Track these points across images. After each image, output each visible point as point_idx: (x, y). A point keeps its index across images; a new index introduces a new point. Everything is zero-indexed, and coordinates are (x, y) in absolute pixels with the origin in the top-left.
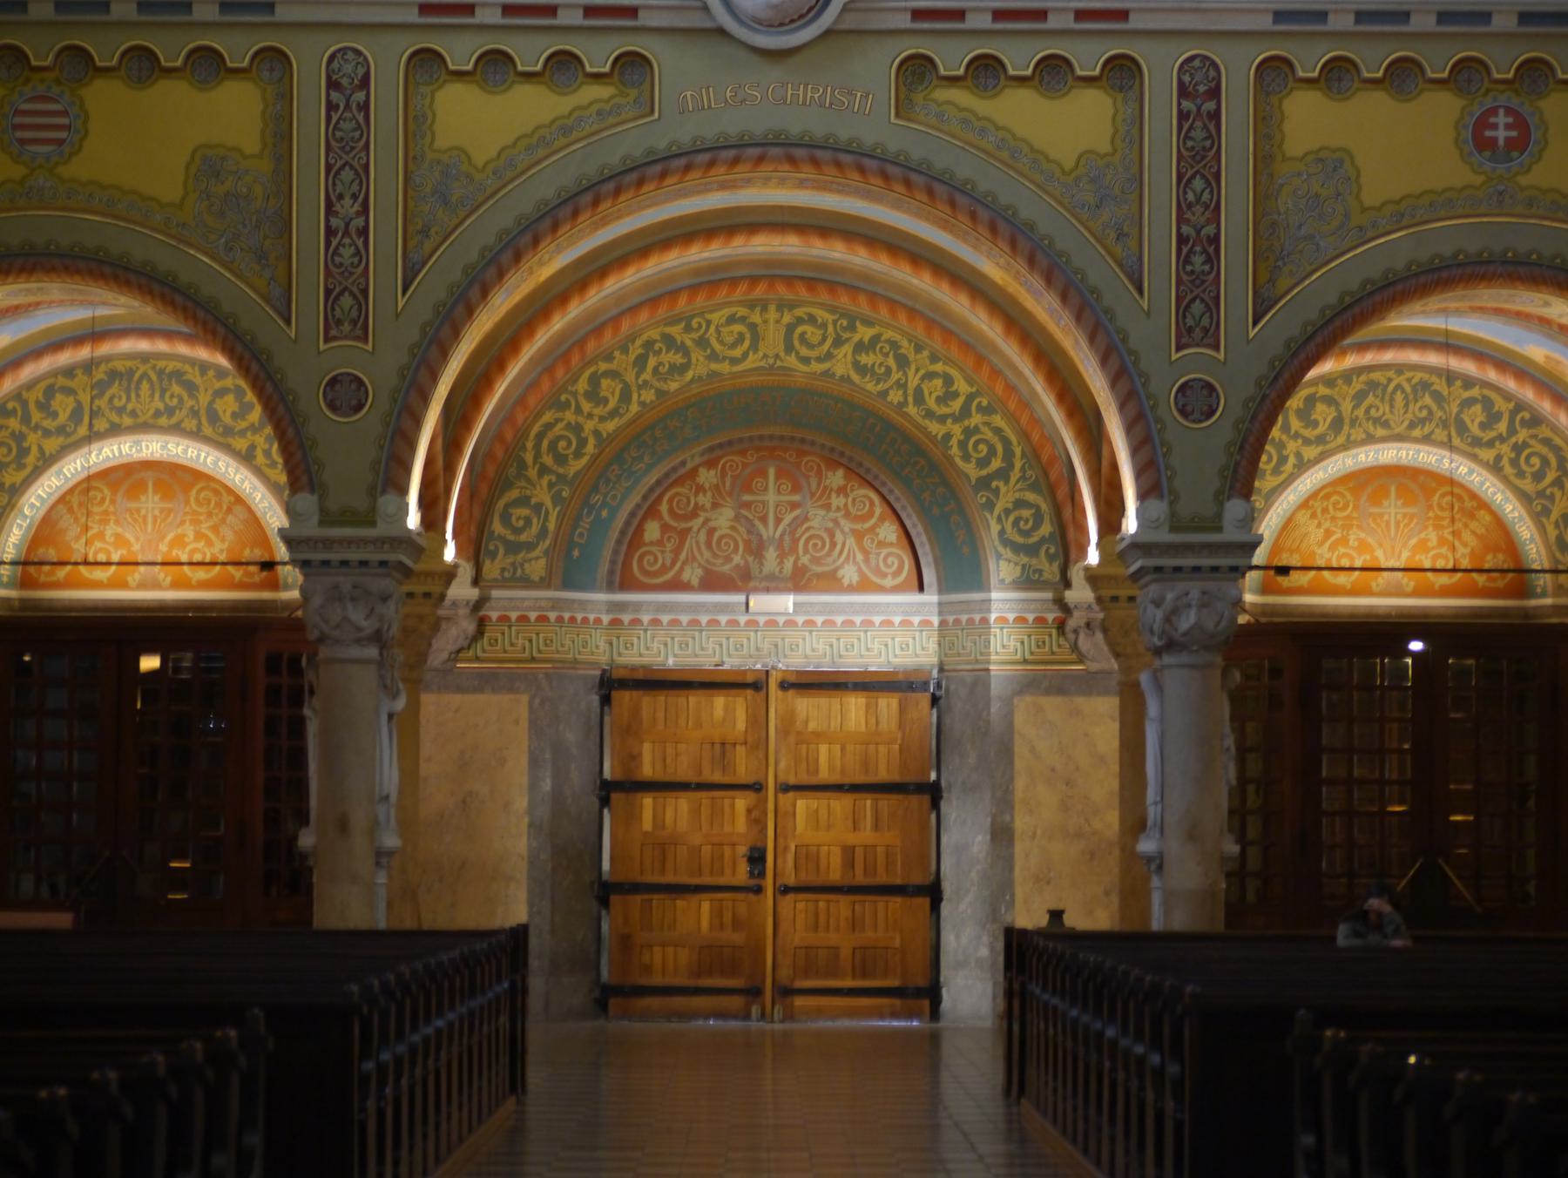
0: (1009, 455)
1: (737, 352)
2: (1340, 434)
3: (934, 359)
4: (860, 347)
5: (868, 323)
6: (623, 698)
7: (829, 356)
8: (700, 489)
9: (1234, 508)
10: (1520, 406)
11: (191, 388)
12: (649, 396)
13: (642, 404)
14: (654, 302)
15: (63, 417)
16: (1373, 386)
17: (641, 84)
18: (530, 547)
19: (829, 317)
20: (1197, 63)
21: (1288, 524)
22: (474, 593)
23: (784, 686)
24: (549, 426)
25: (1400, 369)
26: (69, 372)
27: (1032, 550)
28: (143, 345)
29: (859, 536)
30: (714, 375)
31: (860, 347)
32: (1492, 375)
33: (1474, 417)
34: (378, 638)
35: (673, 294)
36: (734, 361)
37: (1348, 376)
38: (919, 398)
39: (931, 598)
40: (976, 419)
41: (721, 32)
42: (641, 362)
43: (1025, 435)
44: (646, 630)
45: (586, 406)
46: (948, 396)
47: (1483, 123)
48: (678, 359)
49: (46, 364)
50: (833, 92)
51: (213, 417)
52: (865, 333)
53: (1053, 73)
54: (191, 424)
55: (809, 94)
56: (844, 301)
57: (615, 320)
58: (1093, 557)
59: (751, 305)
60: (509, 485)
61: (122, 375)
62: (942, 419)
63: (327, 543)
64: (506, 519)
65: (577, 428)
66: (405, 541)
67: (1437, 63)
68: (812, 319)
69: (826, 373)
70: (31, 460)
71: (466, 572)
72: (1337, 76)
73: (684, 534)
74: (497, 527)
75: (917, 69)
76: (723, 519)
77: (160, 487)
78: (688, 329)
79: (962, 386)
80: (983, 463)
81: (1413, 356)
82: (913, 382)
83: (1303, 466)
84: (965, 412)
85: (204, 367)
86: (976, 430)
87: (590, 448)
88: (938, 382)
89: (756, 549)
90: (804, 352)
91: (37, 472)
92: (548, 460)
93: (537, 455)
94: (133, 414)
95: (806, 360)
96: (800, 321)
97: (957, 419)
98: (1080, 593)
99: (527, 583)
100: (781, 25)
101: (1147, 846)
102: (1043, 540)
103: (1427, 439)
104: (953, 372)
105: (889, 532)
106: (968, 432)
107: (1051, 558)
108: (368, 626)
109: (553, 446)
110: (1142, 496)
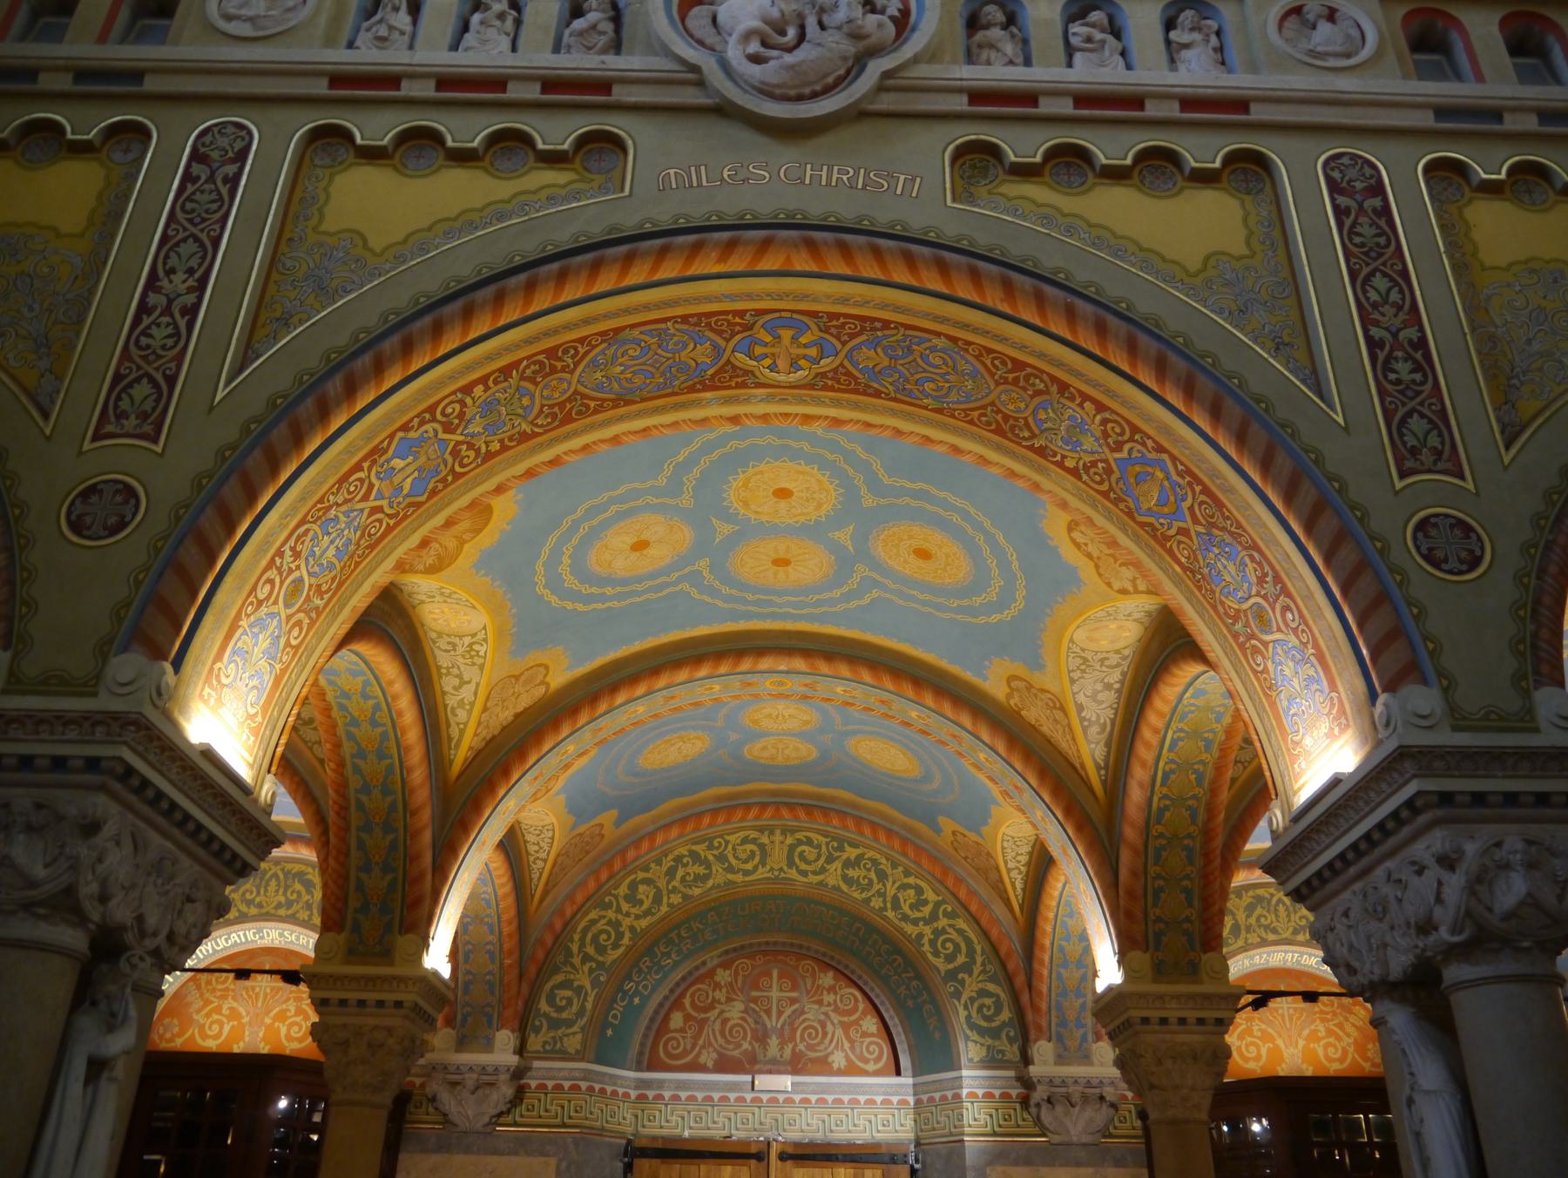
0: (971, 952)
1: (749, 866)
3: (907, 874)
4: (848, 864)
5: (854, 845)
6: (644, 1165)
7: (823, 870)
8: (717, 986)
12: (676, 899)
13: (669, 905)
14: (683, 821)
16: (1259, 899)
17: (611, 170)
18: (569, 1023)
19: (823, 840)
20: (1345, 160)
22: (514, 1060)
23: (783, 1157)
24: (593, 922)
27: (994, 1034)
29: (846, 1027)
30: (731, 882)
31: (848, 864)
35: (699, 816)
36: (746, 873)
38: (896, 905)
39: (907, 1080)
40: (943, 922)
42: (671, 873)
43: (985, 934)
44: (666, 1105)
45: (625, 907)
46: (920, 903)
48: (701, 870)
50: (867, 174)
52: (852, 853)
54: (303, 915)
55: (835, 176)
59: (761, 830)
60: (556, 971)
62: (915, 922)
64: (551, 1001)
65: (616, 924)
68: (809, 842)
69: (821, 883)
73: (702, 1023)
74: (544, 1006)
76: (735, 1011)
78: (711, 847)
79: (930, 895)
80: (950, 958)
82: (891, 891)
84: (934, 917)
86: (944, 931)
87: (626, 941)
88: (912, 892)
89: (762, 1038)
90: (803, 867)
92: (591, 950)
93: (582, 945)
94: (260, 906)
95: (804, 873)
96: (800, 842)
97: (927, 922)
99: (564, 1056)
102: (1004, 1025)
104: (922, 884)
105: (871, 1024)
106: (937, 933)
107: (1011, 1040)
109: (595, 939)
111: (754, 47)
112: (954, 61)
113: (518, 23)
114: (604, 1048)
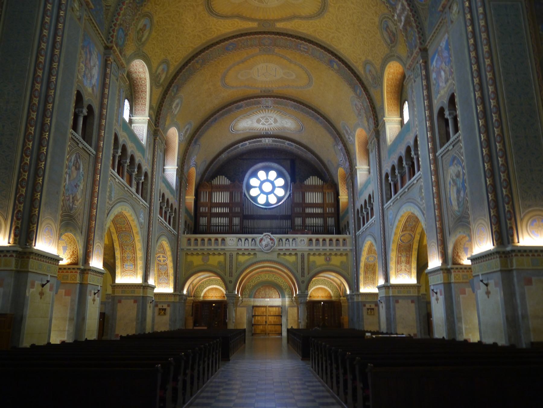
2: (315, 284)
9: (306, 291)
10: (330, 282)
11: (218, 281)
15: (207, 284)
16: (318, 280)
21: (311, 292)
22: (242, 299)
25: (320, 279)
26: (207, 280)
27: (289, 295)
28: (214, 278)
32: (328, 279)
33: (327, 283)
34: (233, 303)
37: (316, 280)
39: (281, 299)
40: (284, 283)
41: (262, 251)
42: (256, 279)
43: (289, 285)
46: (282, 281)
47: (326, 258)
49: (206, 279)
51: (220, 284)
52: (275, 276)
53: (290, 254)
56: (273, 273)
57: (254, 275)
58: (294, 296)
61: (212, 280)
63: (229, 295)
66: (236, 295)
67: (322, 253)
70: (204, 287)
71: (241, 297)
72: (314, 254)
73: (260, 294)
74: (244, 293)
75: (279, 254)
76: (263, 292)
77: (215, 290)
79: (283, 281)
81: (321, 278)
83: (312, 287)
85: (219, 279)
89: (266, 295)
91: (205, 288)
98: (293, 299)
99: (246, 298)
101: (299, 321)
103: (323, 285)
105: (277, 293)
108: (232, 302)
110: (298, 290)
114: (250, 297)
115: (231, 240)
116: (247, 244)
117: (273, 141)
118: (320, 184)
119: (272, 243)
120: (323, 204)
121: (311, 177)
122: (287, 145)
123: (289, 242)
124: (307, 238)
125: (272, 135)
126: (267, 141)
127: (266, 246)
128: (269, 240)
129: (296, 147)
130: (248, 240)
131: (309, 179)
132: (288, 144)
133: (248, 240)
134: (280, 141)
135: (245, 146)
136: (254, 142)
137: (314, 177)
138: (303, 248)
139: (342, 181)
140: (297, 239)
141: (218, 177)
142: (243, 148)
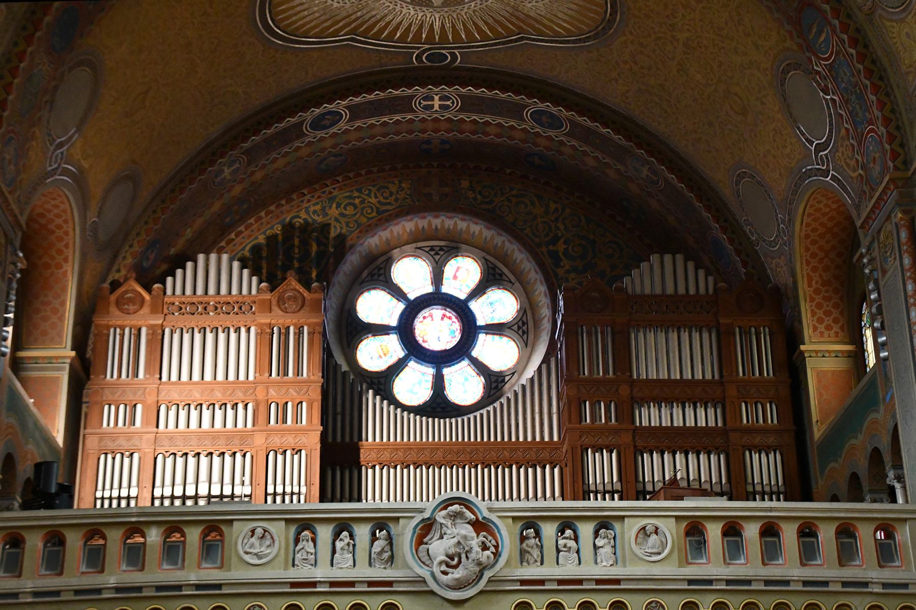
20: (653, 605)
41: (432, 593)
100: (460, 588)
111: (444, 568)
112: (516, 568)
113: (354, 546)
115: (259, 531)
116: (344, 558)
117: (469, 104)
118: (702, 291)
119: (485, 548)
120: (721, 383)
121: (655, 258)
122: (529, 124)
123: (576, 539)
124: (677, 518)
125: (457, 68)
126: (437, 103)
127: (452, 561)
128: (468, 530)
129: (577, 132)
130: (352, 536)
131: (644, 265)
132: (537, 116)
133: (352, 536)
134: (502, 102)
135: (334, 130)
136: (377, 108)
137: (668, 258)
138: (657, 571)
139: (814, 269)
140: (617, 526)
141: (201, 258)
142: (322, 139)
